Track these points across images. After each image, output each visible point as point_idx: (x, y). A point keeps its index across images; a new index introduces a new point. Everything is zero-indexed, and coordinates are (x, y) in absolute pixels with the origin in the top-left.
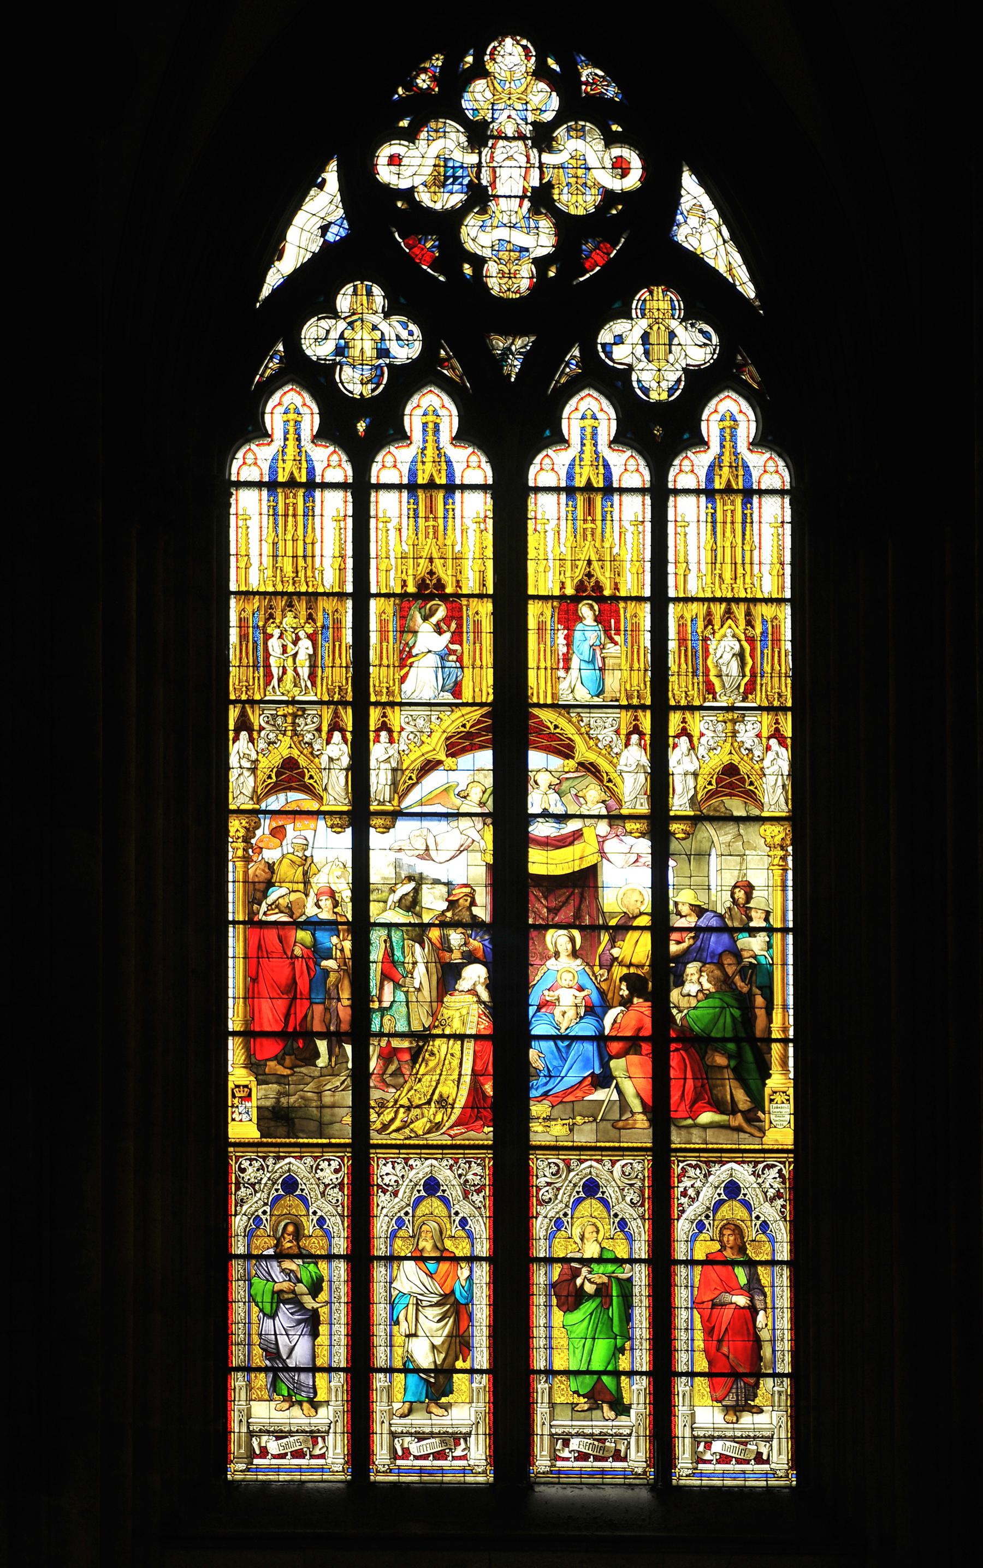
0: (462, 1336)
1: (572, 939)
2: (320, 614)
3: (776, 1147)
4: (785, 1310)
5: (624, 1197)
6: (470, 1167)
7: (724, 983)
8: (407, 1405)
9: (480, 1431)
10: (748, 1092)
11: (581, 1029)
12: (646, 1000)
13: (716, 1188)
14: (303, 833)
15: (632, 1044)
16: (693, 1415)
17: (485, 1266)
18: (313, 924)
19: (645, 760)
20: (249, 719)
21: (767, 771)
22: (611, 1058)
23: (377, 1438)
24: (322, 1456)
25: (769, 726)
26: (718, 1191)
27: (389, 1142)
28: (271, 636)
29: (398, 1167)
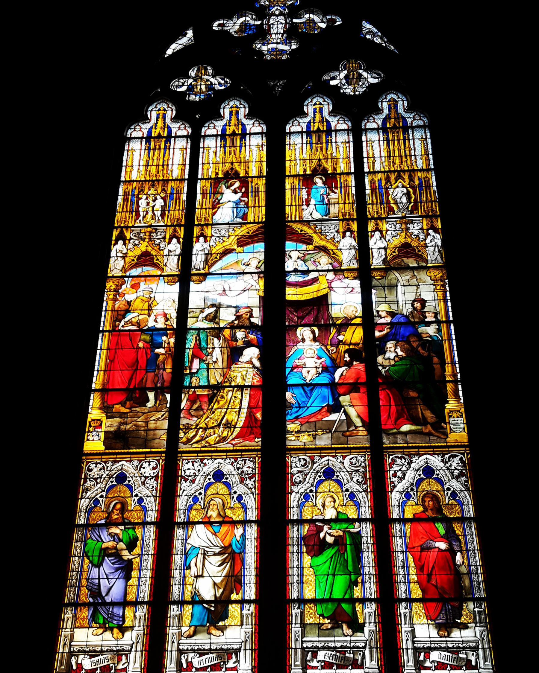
0: (237, 576)
3: (456, 444)
4: (477, 552)
5: (352, 479)
6: (245, 463)
7: (411, 352)
8: (192, 628)
9: (248, 648)
10: (433, 412)
11: (320, 380)
12: (361, 363)
13: (417, 471)
14: (151, 286)
15: (353, 388)
16: (413, 632)
17: (255, 527)
19: (354, 243)
22: (340, 395)
23: (168, 655)
27: (191, 449)
28: (141, 198)
29: (196, 465)
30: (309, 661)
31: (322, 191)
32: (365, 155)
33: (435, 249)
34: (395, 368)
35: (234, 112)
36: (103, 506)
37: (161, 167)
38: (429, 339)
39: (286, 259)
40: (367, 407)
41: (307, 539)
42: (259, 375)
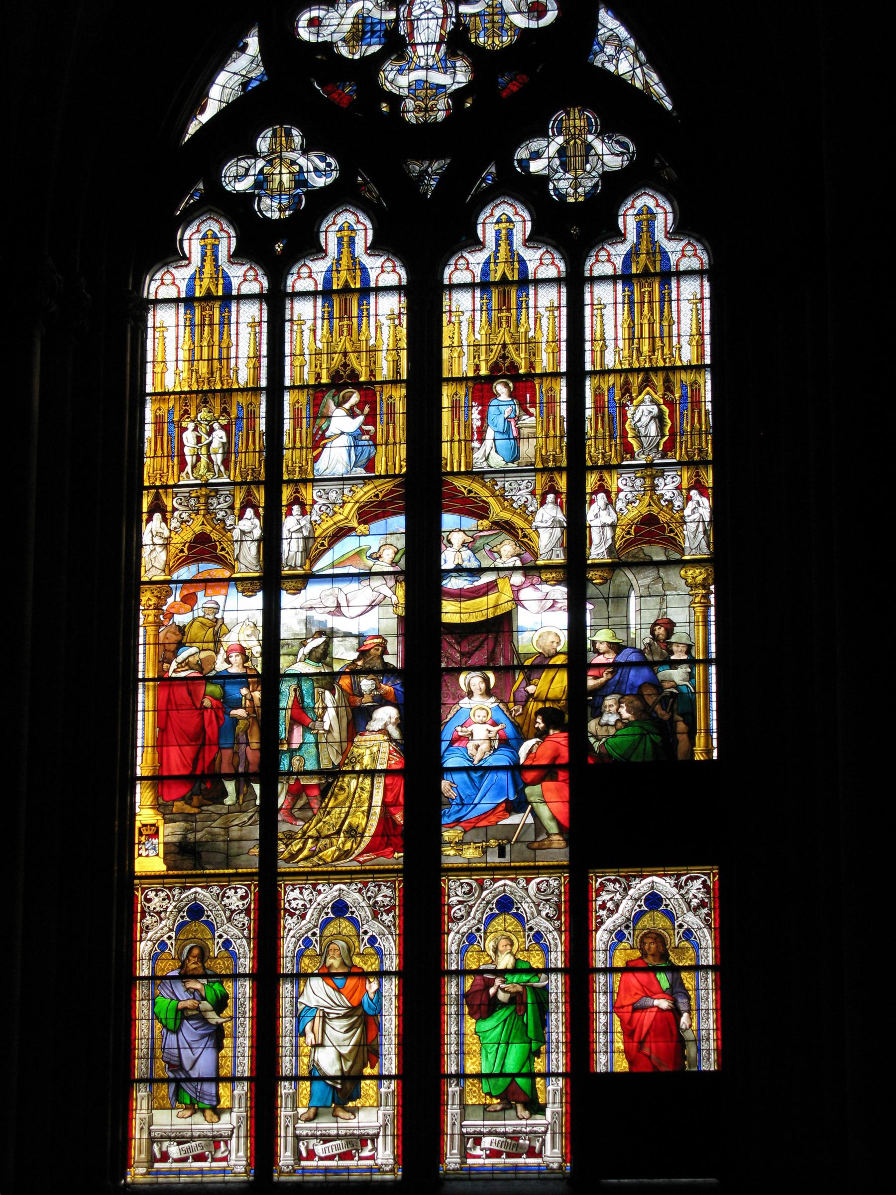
0: (370, 1045)
1: (486, 680)
2: (234, 408)
4: (711, 1012)
6: (379, 890)
7: (644, 713)
8: (312, 1110)
9: (389, 1132)
11: (495, 760)
12: (562, 732)
13: (637, 900)
14: (214, 598)
15: (547, 772)
17: (395, 981)
18: (224, 678)
19: (561, 517)
20: (163, 502)
21: (688, 519)
22: (526, 785)
23: (281, 1142)
24: (225, 1159)
25: (689, 479)
26: (639, 903)
27: (297, 870)
28: (186, 429)
29: (306, 892)
30: (470, 1149)
31: (507, 411)
32: (588, 335)
33: (698, 527)
34: (617, 740)
35: (346, 239)
36: (173, 951)
37: (216, 364)
38: (675, 691)
39: (443, 546)
40: (567, 804)
41: (470, 996)
42: (398, 753)
